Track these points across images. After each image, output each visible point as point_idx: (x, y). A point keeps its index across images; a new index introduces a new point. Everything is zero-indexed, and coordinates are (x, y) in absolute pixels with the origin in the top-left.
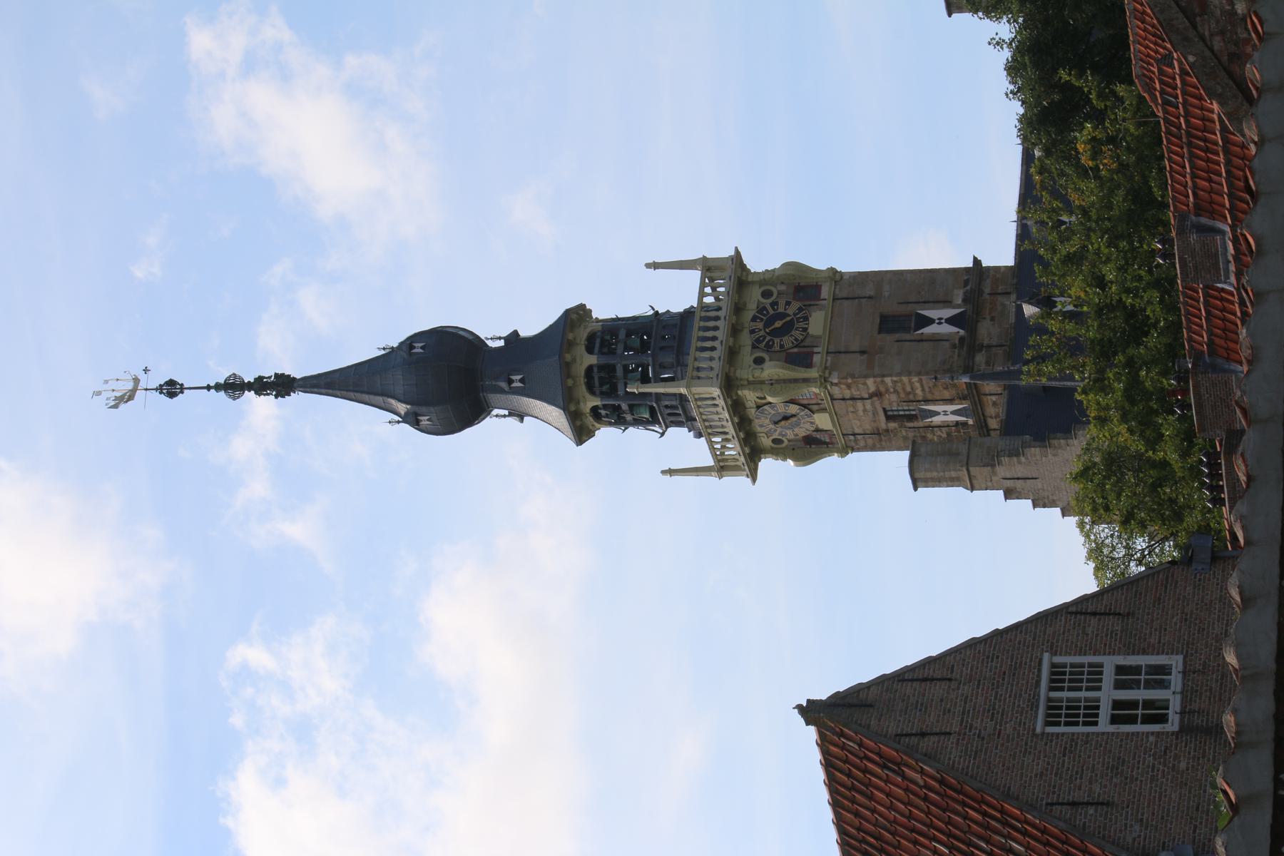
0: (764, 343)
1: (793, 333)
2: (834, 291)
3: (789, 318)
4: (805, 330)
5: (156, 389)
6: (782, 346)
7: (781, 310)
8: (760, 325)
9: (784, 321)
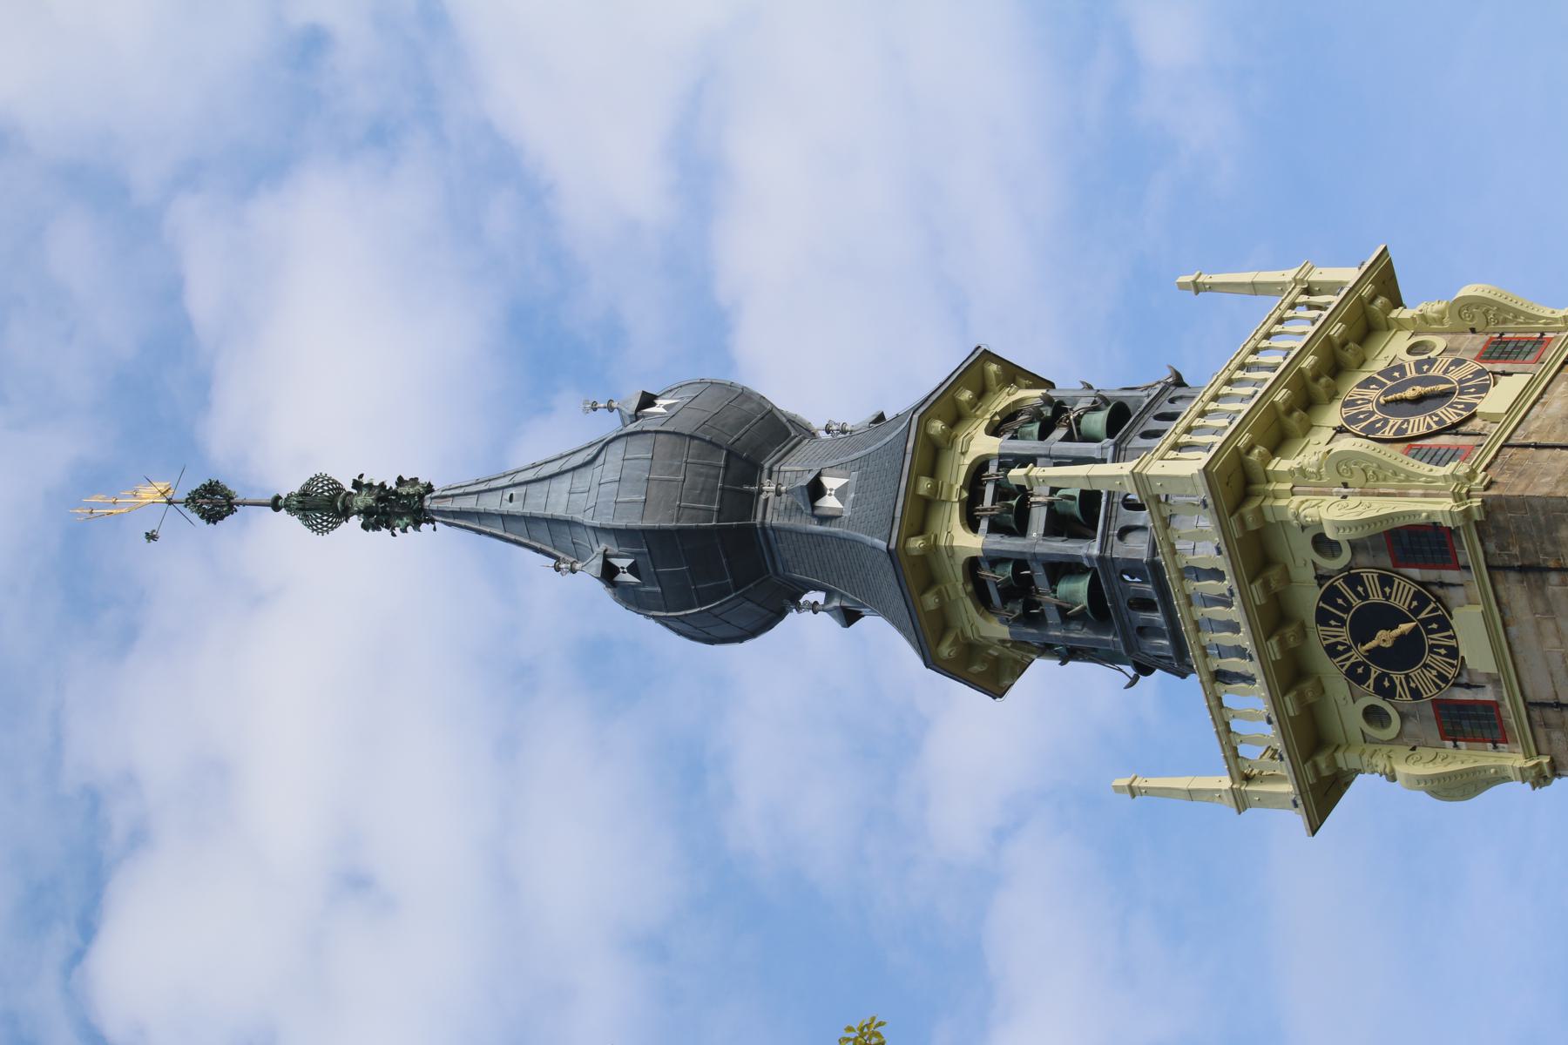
0: (1371, 681)
1: (1427, 659)
2: (1485, 553)
3: (1405, 627)
4: (1453, 652)
5: (187, 503)
6: (1416, 694)
7: (1376, 597)
8: (1344, 635)
9: (1396, 632)
